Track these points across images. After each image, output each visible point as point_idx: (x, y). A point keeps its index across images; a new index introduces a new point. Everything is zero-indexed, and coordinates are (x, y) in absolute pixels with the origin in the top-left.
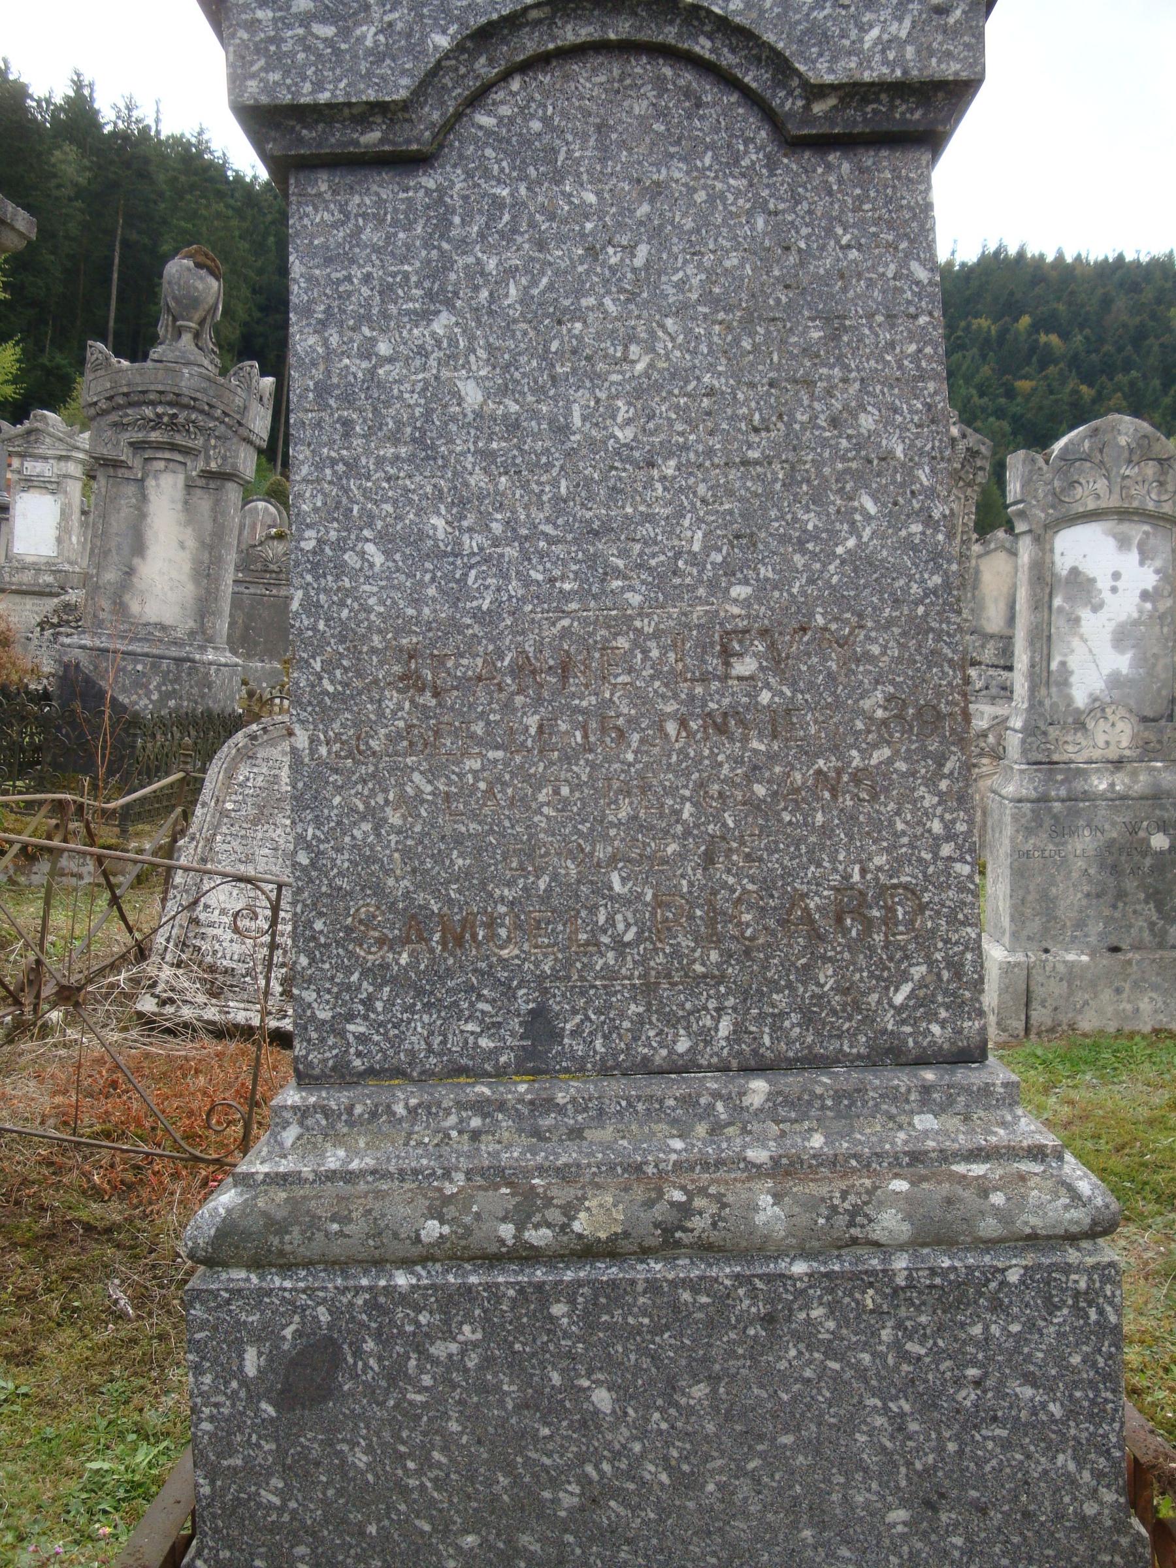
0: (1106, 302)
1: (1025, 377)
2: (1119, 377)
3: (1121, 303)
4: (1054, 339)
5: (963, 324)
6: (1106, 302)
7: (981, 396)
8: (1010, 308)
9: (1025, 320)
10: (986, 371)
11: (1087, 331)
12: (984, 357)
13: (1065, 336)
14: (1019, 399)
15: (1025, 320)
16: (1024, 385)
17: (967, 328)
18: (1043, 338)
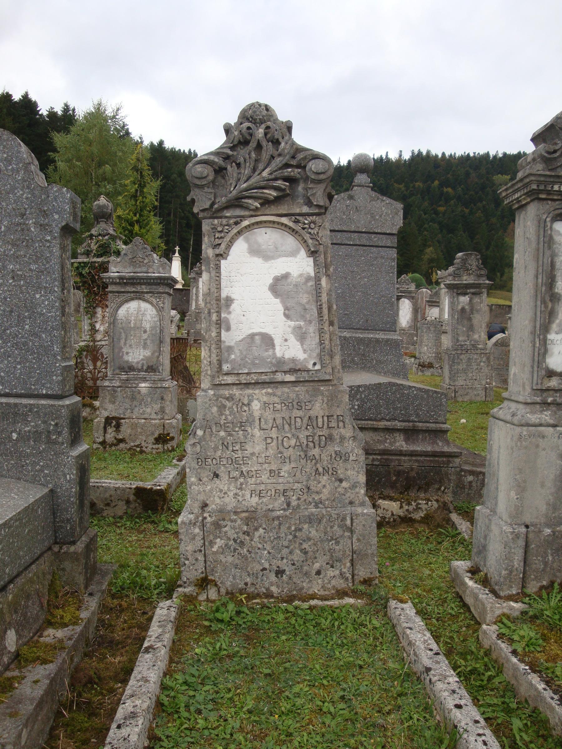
0: (467, 174)
1: (440, 206)
2: (479, 205)
3: (473, 175)
4: (450, 190)
5: (412, 185)
6: (467, 174)
7: (425, 214)
8: (429, 178)
9: (436, 183)
10: (426, 204)
11: (462, 186)
12: (423, 198)
13: (454, 188)
14: (441, 215)
15: (436, 183)
16: (442, 209)
17: (414, 186)
18: (445, 190)
